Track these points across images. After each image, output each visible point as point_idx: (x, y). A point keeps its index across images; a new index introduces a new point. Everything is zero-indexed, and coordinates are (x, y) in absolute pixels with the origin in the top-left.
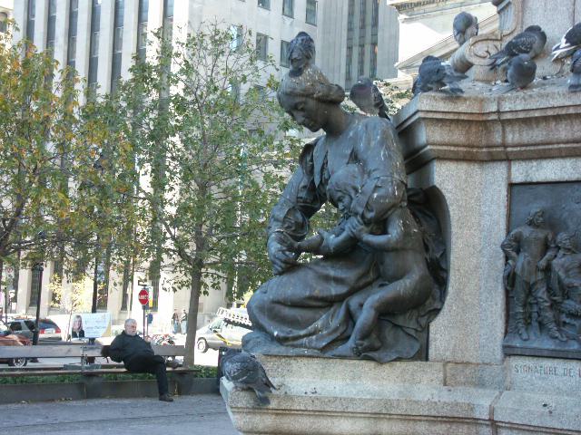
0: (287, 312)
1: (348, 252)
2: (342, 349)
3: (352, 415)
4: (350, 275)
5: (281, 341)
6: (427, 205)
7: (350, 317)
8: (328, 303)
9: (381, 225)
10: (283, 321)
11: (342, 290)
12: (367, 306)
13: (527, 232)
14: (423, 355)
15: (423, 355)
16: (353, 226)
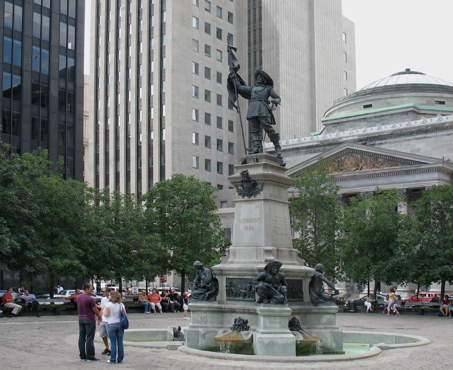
0: (196, 295)
1: (204, 287)
2: (204, 300)
3: (206, 308)
4: (205, 290)
5: (196, 299)
6: (215, 281)
7: (205, 295)
8: (202, 294)
9: (208, 284)
10: (196, 296)
11: (203, 292)
12: (207, 294)
13: (228, 284)
14: (215, 300)
15: (215, 300)
16: (204, 284)
